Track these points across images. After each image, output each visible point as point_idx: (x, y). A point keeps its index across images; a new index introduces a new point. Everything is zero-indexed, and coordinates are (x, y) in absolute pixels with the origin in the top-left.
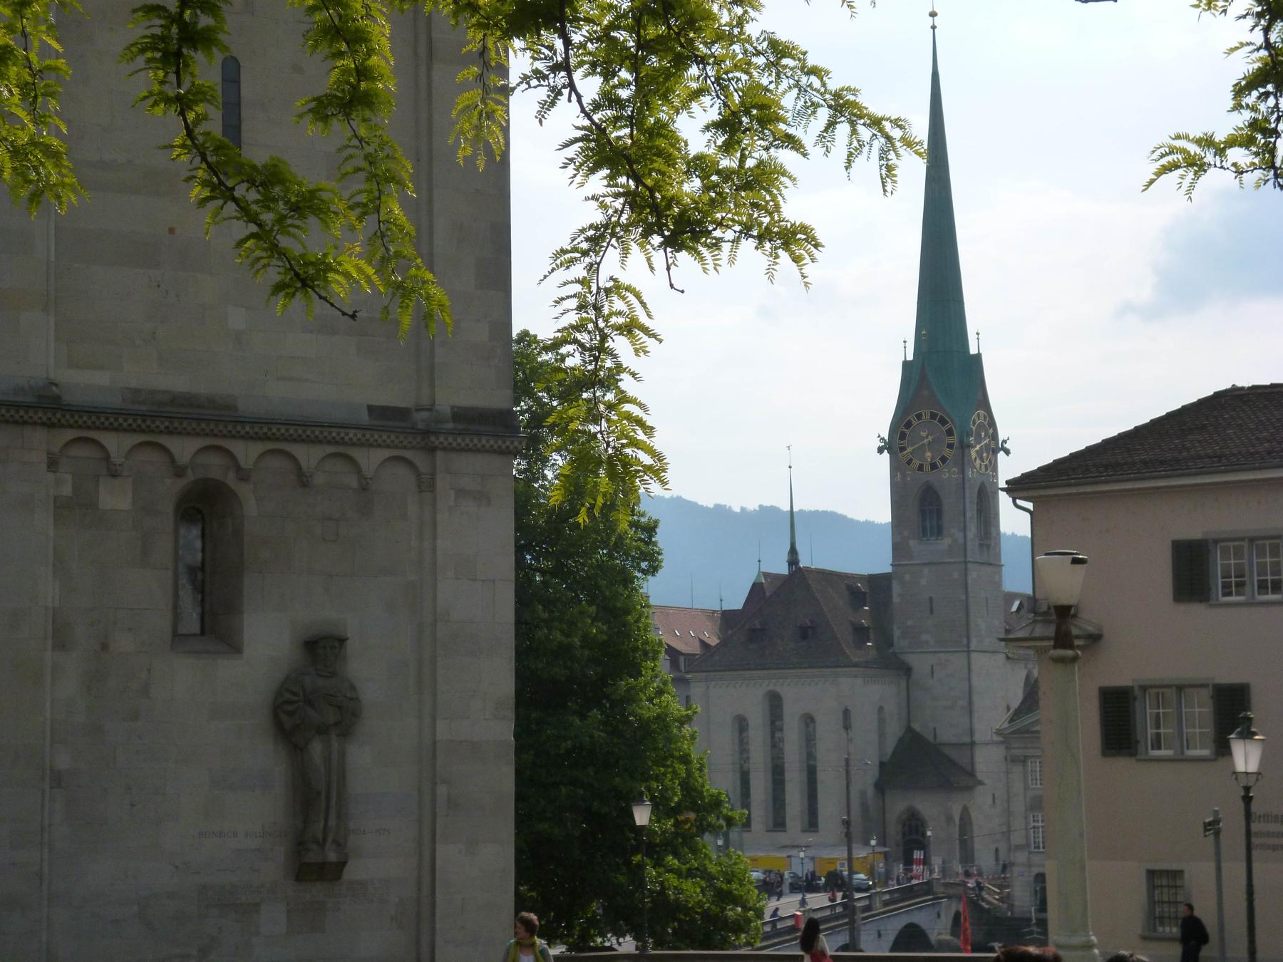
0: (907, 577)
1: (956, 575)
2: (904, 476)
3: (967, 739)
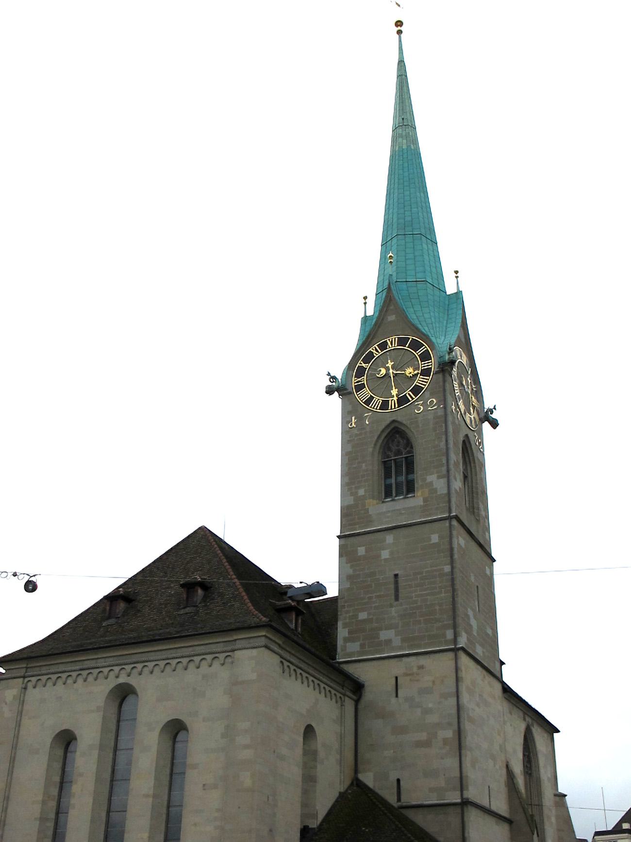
0: (361, 551)
1: (435, 538)
2: (360, 419)
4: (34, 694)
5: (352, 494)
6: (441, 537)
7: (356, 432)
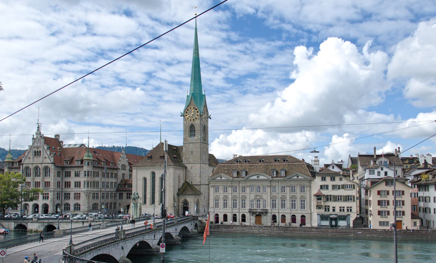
0: (187, 146)
1: (198, 145)
2: (186, 122)
3: (199, 184)
4: (139, 172)
7: (186, 124)
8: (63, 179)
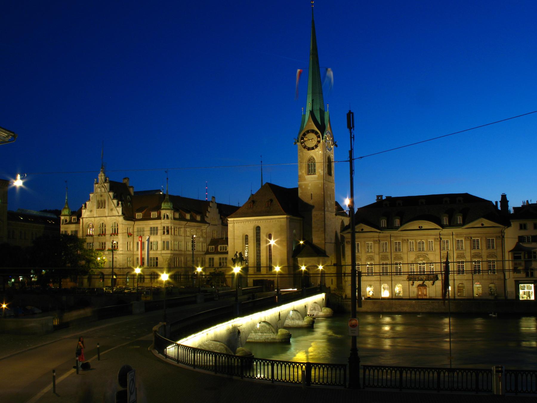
5: (301, 172)
6: (322, 185)
8: (134, 237)
